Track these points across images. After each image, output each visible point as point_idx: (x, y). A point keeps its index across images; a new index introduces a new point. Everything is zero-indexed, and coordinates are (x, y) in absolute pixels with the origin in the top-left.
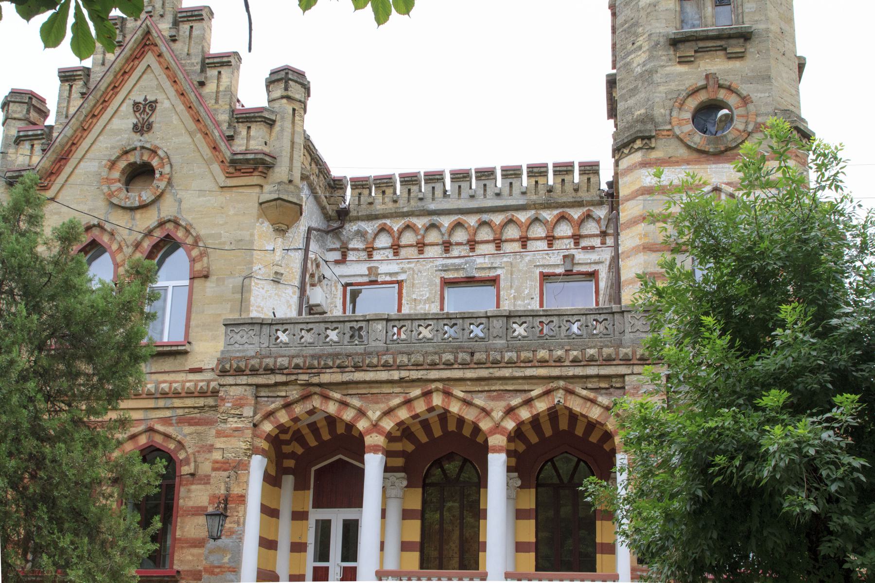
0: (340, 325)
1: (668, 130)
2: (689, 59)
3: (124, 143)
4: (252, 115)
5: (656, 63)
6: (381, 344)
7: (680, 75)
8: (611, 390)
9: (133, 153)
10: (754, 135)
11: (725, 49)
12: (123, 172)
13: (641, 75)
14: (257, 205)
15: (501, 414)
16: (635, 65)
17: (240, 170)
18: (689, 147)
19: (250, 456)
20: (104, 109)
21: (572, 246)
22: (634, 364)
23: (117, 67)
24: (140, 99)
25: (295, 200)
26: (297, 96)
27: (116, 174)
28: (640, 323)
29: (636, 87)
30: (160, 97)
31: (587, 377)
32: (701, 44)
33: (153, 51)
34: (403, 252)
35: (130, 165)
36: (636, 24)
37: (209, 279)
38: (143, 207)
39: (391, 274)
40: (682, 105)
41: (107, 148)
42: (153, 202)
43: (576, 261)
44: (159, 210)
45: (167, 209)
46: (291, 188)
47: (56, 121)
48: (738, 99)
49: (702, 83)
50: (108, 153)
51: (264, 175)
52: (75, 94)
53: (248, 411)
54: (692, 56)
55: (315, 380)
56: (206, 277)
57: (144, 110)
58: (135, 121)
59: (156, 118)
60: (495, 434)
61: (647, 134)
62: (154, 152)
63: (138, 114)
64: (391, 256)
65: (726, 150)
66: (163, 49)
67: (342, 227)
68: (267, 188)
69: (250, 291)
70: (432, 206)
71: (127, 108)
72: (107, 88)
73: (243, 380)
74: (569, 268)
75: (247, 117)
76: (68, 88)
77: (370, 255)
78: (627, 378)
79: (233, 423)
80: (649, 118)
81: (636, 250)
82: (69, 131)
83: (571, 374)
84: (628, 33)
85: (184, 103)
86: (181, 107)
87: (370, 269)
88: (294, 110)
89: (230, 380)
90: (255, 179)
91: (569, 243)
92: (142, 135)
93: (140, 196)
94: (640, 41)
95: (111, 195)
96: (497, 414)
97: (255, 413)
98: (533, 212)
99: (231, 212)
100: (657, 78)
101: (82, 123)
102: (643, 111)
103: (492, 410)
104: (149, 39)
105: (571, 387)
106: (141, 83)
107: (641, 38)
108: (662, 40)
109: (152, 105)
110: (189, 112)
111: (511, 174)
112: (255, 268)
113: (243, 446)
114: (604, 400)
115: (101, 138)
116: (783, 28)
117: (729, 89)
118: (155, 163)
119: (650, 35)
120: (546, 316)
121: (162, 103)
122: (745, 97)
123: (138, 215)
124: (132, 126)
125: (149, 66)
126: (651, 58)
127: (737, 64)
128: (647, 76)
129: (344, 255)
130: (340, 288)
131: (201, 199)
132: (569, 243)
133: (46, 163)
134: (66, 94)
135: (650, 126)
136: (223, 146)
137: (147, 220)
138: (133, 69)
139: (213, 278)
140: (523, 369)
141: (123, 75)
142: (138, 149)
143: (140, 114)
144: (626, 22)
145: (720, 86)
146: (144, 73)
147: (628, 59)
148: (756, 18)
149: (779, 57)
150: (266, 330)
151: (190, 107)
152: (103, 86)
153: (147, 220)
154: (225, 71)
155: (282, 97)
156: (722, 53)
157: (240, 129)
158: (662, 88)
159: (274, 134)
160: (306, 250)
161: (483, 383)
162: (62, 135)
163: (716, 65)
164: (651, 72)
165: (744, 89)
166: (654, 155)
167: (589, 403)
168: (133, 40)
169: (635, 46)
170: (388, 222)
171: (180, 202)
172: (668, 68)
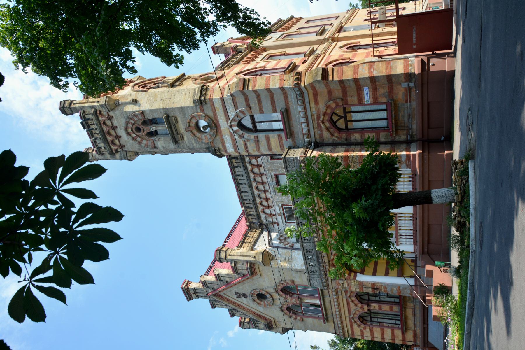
0: (306, 256)
6: (311, 244)
7: (188, 139)
12: (261, 301)
19: (357, 281)
23: (227, 303)
24: (236, 296)
25: (261, 255)
26: (224, 254)
27: (262, 303)
30: (234, 291)
32: (175, 133)
34: (271, 204)
35: (258, 299)
38: (272, 297)
39: (280, 209)
42: (270, 294)
45: (271, 290)
46: (257, 257)
49: (190, 132)
51: (254, 264)
53: (341, 282)
55: (327, 264)
56: (293, 281)
58: (243, 298)
59: (241, 292)
64: (273, 208)
67: (265, 225)
68: (258, 264)
69: (296, 269)
71: (239, 299)
73: (330, 283)
77: (274, 215)
79: (346, 285)
87: (279, 215)
89: (331, 287)
90: (256, 267)
95: (269, 305)
97: (341, 280)
109: (237, 293)
112: (288, 267)
113: (353, 283)
117: (190, 122)
118: (256, 293)
126: (184, 148)
127: (179, 119)
129: (275, 223)
130: (287, 224)
137: (276, 296)
138: (226, 298)
139: (294, 279)
145: (189, 126)
149: (172, 101)
150: (311, 276)
152: (234, 307)
153: (276, 296)
154: (221, 276)
158: (195, 145)
160: (278, 247)
163: (182, 127)
166: (221, 147)
170: (260, 210)
171: (268, 287)
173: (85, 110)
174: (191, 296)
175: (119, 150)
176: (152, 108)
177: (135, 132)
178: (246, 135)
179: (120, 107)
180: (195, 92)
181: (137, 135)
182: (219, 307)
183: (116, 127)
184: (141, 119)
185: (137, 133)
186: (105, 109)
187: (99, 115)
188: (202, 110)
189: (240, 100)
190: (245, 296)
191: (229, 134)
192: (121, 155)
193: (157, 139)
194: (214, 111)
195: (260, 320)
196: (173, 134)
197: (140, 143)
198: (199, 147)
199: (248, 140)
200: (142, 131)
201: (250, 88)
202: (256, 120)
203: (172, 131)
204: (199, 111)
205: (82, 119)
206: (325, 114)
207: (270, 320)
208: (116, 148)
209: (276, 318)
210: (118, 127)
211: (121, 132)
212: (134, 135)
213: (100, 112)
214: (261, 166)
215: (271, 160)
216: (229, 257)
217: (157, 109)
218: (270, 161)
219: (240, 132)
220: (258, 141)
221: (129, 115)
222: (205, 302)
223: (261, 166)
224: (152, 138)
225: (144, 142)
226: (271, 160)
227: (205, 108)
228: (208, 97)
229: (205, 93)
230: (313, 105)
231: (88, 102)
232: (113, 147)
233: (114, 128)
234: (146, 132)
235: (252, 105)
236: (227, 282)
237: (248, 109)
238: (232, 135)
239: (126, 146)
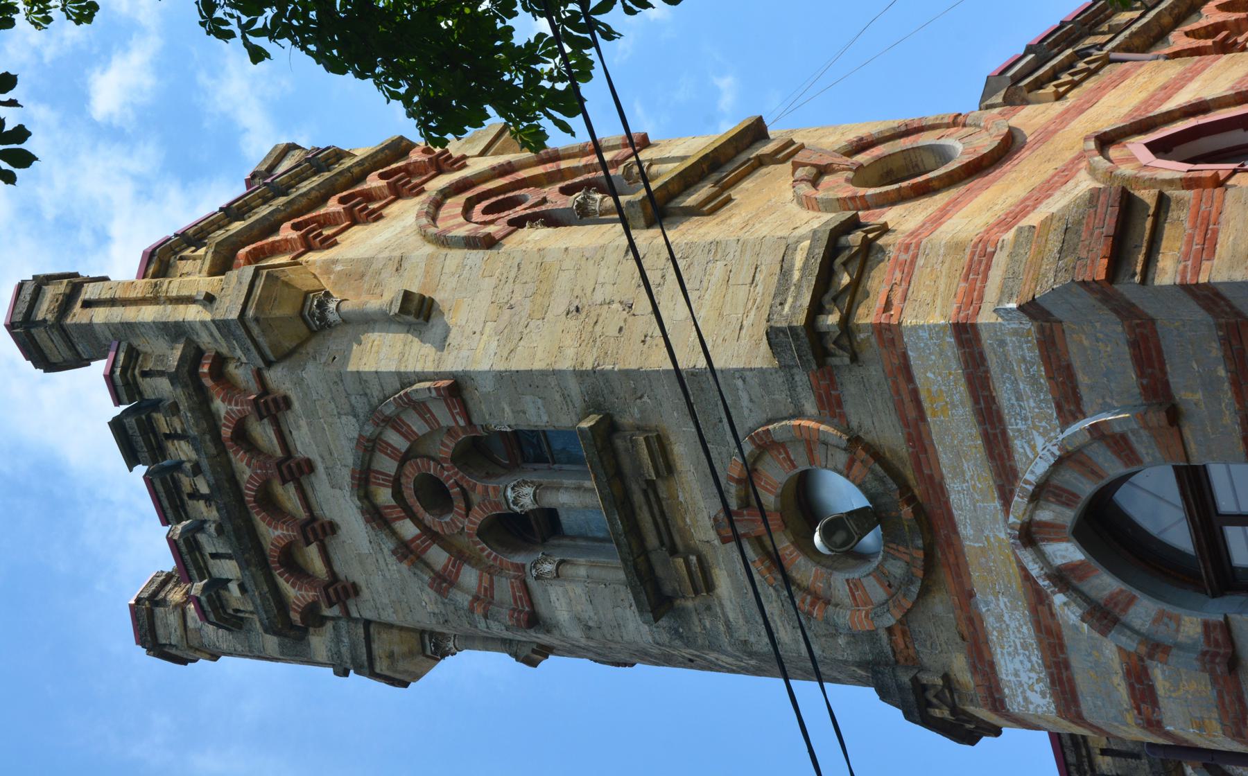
10: (854, 423)
11: (651, 484)
18: (925, 591)
32: (652, 540)
48: (767, 458)
54: (687, 563)
65: (911, 500)
116: (563, 308)
122: (758, 446)
148: (557, 397)
163: (696, 504)
172: (731, 616)
173: (141, 344)
176: (519, 363)
177: (418, 508)
178: (1144, 611)
179: (333, 344)
180: (785, 273)
181: (426, 530)
183: (308, 467)
184: (450, 431)
185: (428, 518)
186: (246, 351)
187: (208, 382)
188: (831, 405)
189: (1100, 348)
191: (1016, 583)
192: (337, 640)
193: (548, 567)
194: (912, 414)
196: (644, 551)
197: (444, 582)
199: (1157, 648)
200: (459, 504)
201: (1168, 271)
203: (634, 528)
204: (810, 407)
205: (118, 402)
208: (310, 595)
210: (320, 467)
211: (338, 503)
212: (408, 529)
213: (220, 362)
217: (543, 373)
219: (1105, 584)
220: (1233, 663)
221: (376, 393)
224: (519, 559)
225: (470, 577)
228: (868, 315)
229: (856, 284)
231: (154, 300)
232: (294, 593)
233: (298, 471)
234: (478, 516)
235: (1188, 394)
237: (1158, 418)
238: (1038, 601)
239: (365, 593)
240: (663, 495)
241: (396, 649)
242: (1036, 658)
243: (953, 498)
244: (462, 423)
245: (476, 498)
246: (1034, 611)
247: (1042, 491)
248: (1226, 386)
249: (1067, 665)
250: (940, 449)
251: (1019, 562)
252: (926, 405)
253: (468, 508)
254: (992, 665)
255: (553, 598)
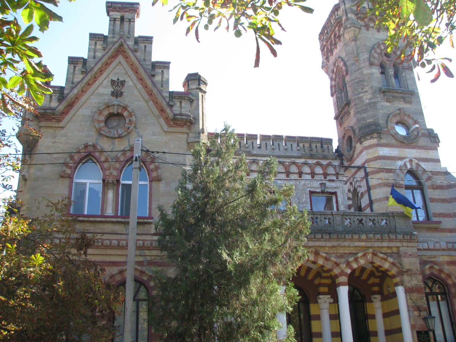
1: (386, 131)
2: (390, 100)
3: (106, 101)
4: (183, 96)
5: (377, 100)
8: (393, 254)
9: (112, 107)
13: (369, 104)
14: (186, 143)
15: (345, 265)
16: (364, 98)
17: (177, 124)
18: (396, 140)
20: (95, 81)
21: (323, 179)
22: (403, 242)
24: (115, 79)
27: (103, 118)
28: (402, 222)
29: (367, 109)
30: (127, 79)
31: (382, 247)
33: (123, 55)
36: (363, 81)
37: (161, 182)
38: (120, 137)
40: (391, 120)
41: (96, 103)
43: (326, 187)
44: (129, 140)
47: (66, 84)
49: (398, 112)
50: (96, 105)
51: (189, 128)
52: (77, 72)
56: (160, 180)
57: (118, 85)
58: (113, 90)
60: (342, 276)
61: (379, 132)
62: (125, 108)
63: (114, 87)
66: (131, 55)
68: (191, 135)
70: (255, 152)
72: (98, 70)
74: (323, 190)
75: (180, 96)
76: (73, 67)
78: (400, 248)
80: (376, 124)
81: (380, 185)
82: (75, 91)
83: (376, 245)
84: (358, 84)
85: (142, 84)
86: (140, 86)
88: (202, 96)
90: (185, 129)
91: (322, 177)
92: (117, 98)
93: (117, 132)
94: (366, 89)
96: (343, 266)
98: (304, 160)
99: (172, 146)
100: (378, 106)
101: (82, 88)
102: (372, 120)
103: (340, 263)
104: (121, 48)
105: (375, 252)
106: (115, 71)
107: (367, 87)
108: (377, 90)
109: (123, 83)
110: (145, 89)
111: (292, 140)
114: (390, 260)
115: (92, 97)
117: (409, 116)
118: (125, 114)
119: (372, 87)
120: (359, 216)
121: (128, 83)
123: (116, 141)
124: (110, 93)
125: (120, 62)
128: (373, 105)
131: (154, 137)
132: (322, 177)
133: (61, 107)
134: (72, 70)
135: (378, 128)
136: (168, 110)
138: (111, 63)
139: (163, 182)
140: (354, 243)
141: (106, 65)
142: (116, 105)
143: (115, 87)
144: (355, 79)
145: (405, 115)
146: (117, 65)
147: (360, 95)
151: (146, 87)
152: (96, 69)
154: (165, 71)
155: (197, 89)
156: (402, 100)
157: (176, 102)
158: (381, 111)
159: (193, 107)
161: (334, 249)
162: (72, 93)
163: (402, 105)
164: (375, 103)
165: (416, 117)
166: (383, 141)
167: (383, 260)
168: (113, 48)
169: (363, 90)
172: (382, 103)
174: (118, 11)
175: (362, 23)
182: (90, 44)
190: (116, 94)
195: (64, 104)
198: (380, 116)
200: (388, 59)
202: (414, 191)
206: (441, 271)
207: (59, 121)
209: (62, 132)
214: (300, 177)
215: (310, 191)
216: (200, 94)
218: (308, 190)
222: (103, 27)
223: (300, 177)
225: (376, 55)
226: (310, 191)
227: (428, 139)
230: (446, 259)
235: (437, 192)
236: (154, 76)
238: (401, 159)
239: (367, 32)
240: (401, 99)
241: (356, 32)
242: (389, 155)
243: (412, 150)
244: (405, 67)
245: (390, 62)
246: (397, 157)
247: (418, 165)
248: (439, 198)
249: (389, 160)
250: (420, 150)
251: (406, 158)
252: (427, 151)
253: (388, 61)
254: (385, 147)
255: (376, 70)
